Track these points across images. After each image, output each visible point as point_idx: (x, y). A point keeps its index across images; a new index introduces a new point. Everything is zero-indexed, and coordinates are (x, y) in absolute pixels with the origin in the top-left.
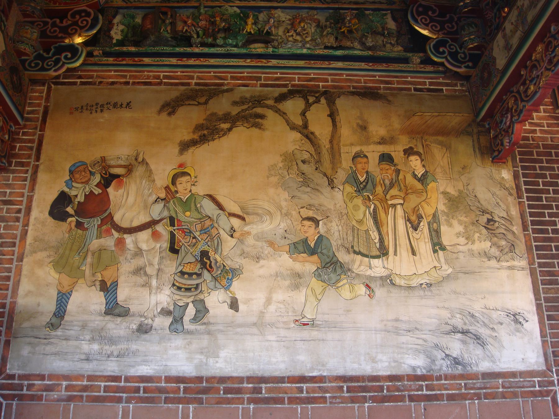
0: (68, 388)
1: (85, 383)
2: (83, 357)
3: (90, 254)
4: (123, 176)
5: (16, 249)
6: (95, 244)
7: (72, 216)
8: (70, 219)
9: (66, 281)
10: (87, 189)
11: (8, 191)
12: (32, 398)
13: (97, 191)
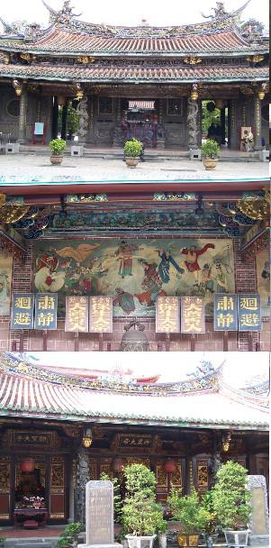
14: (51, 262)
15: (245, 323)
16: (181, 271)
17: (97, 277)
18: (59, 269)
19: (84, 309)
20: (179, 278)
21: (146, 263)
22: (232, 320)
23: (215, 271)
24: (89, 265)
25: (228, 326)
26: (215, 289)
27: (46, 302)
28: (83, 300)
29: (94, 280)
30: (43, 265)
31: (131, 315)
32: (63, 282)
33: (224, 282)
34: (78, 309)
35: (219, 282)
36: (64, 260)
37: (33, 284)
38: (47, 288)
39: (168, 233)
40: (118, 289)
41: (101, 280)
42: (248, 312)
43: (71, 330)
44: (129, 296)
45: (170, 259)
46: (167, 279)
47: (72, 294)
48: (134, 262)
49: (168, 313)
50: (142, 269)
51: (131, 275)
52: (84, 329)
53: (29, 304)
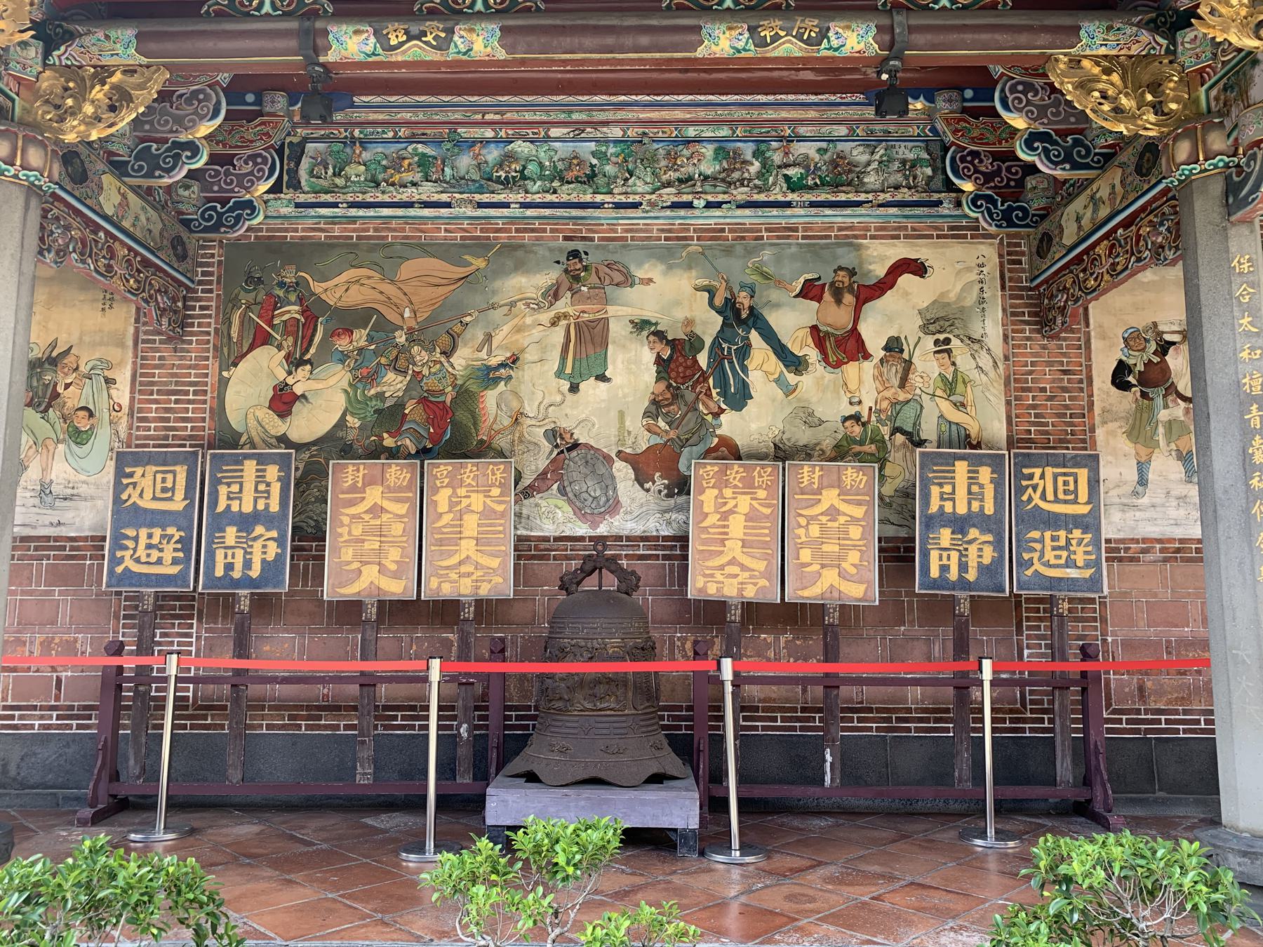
0: (1162, 550)
1: (1177, 545)
2: (1172, 522)
3: (1160, 425)
4: (1178, 343)
5: (1086, 420)
6: (1163, 415)
7: (1135, 386)
8: (1133, 389)
9: (1144, 451)
10: (1145, 357)
11: (1065, 360)
12: (1131, 559)
13: (1156, 359)
14: (290, 328)
15: (1037, 566)
16: (796, 364)
17: (474, 388)
18: (327, 353)
19: (402, 509)
20: (789, 391)
21: (660, 335)
22: (988, 555)
23: (927, 365)
24: (446, 339)
25: (971, 576)
26: (929, 430)
27: (249, 487)
28: (398, 472)
29: (465, 397)
30: (262, 339)
31: (602, 530)
32: (340, 402)
33: (961, 406)
34: (376, 510)
35: (946, 407)
36: (348, 320)
37: (219, 411)
38: (277, 426)
39: (747, 217)
40: (554, 434)
41: (490, 399)
42: (1052, 521)
43: (350, 591)
44: (597, 460)
45: (755, 320)
46: (740, 398)
47: (376, 452)
48: (618, 329)
49: (737, 526)
50: (648, 357)
51: (602, 378)
52: (397, 588)
53: (180, 494)
